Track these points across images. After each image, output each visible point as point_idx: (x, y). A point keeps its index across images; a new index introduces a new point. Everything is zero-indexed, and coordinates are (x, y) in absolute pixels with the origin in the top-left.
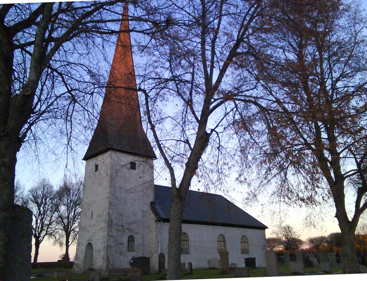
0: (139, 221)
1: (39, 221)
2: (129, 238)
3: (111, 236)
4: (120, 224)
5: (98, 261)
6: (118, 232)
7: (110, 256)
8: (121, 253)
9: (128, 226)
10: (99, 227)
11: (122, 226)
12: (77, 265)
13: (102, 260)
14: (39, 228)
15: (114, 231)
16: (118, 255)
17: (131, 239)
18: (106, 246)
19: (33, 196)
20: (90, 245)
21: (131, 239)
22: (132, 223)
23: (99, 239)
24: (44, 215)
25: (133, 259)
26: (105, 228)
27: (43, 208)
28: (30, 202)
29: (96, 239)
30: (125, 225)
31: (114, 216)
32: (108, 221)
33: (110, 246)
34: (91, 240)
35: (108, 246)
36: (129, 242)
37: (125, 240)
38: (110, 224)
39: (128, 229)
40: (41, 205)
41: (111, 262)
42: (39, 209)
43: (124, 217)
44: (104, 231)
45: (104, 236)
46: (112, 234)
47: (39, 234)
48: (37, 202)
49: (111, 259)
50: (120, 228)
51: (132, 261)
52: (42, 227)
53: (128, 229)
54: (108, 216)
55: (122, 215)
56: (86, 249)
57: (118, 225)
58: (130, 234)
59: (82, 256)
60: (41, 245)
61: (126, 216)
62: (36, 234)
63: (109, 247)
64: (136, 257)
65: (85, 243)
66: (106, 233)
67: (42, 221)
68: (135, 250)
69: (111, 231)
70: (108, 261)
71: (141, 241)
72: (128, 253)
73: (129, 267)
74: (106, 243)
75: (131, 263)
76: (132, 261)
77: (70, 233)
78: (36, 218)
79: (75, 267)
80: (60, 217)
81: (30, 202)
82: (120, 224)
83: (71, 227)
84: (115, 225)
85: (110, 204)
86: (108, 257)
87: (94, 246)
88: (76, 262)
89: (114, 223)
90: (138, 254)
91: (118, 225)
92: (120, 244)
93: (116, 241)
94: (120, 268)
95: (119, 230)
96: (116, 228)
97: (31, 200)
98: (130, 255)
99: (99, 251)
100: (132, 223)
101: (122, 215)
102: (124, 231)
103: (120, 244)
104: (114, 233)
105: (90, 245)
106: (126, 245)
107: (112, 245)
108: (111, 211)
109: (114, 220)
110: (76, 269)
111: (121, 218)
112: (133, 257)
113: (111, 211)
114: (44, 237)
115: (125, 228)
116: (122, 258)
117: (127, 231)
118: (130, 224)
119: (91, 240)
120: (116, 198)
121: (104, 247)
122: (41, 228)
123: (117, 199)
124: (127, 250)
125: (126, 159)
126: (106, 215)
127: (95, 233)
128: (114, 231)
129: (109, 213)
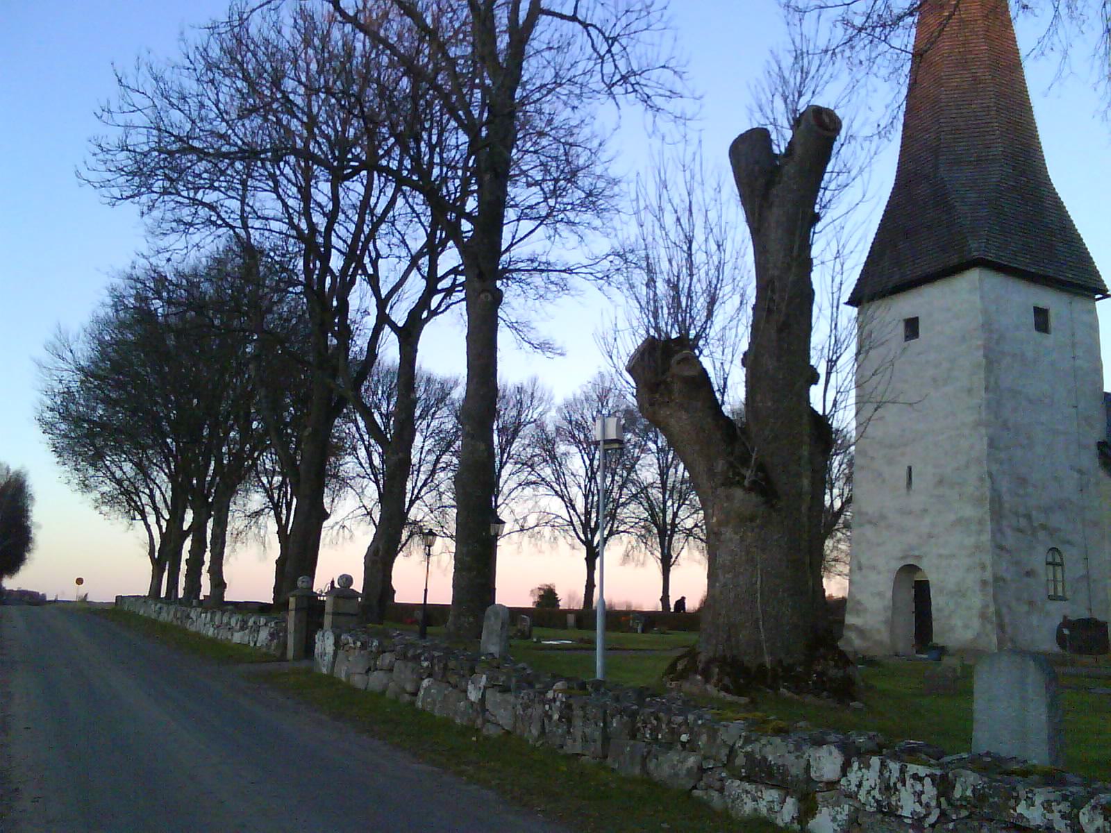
3: (1000, 548)
4: (1021, 510)
7: (1004, 610)
8: (1031, 603)
11: (1028, 517)
13: (976, 623)
15: (1008, 532)
16: (1026, 608)
18: (988, 575)
23: (953, 556)
25: (1066, 623)
26: (981, 522)
30: (1034, 513)
31: (1004, 485)
32: (992, 501)
33: (1004, 580)
35: (997, 579)
37: (1038, 560)
38: (997, 510)
39: (1043, 527)
41: (1009, 629)
43: (1030, 490)
44: (980, 532)
45: (978, 547)
46: (1004, 544)
49: (1007, 620)
50: (1023, 522)
53: (1043, 527)
54: (988, 483)
55: (1022, 481)
57: (1017, 514)
61: (1035, 486)
63: (1001, 584)
66: (986, 537)
68: (1068, 595)
69: (1000, 531)
70: (1001, 627)
72: (1053, 607)
73: (1056, 648)
74: (989, 569)
75: (1061, 639)
82: (1021, 510)
85: (992, 444)
86: (998, 614)
89: (1007, 506)
90: (1078, 611)
91: (1017, 514)
95: (1020, 530)
98: (1057, 612)
99: (960, 593)
104: (1010, 540)
107: (1008, 576)
108: (994, 468)
109: (1006, 498)
111: (1022, 492)
112: (1065, 617)
113: (994, 468)
116: (1035, 620)
117: (1042, 535)
118: (1047, 510)
120: (1005, 426)
121: (984, 583)
123: (1008, 429)
126: (982, 480)
127: (930, 536)
128: (1008, 532)
129: (990, 475)
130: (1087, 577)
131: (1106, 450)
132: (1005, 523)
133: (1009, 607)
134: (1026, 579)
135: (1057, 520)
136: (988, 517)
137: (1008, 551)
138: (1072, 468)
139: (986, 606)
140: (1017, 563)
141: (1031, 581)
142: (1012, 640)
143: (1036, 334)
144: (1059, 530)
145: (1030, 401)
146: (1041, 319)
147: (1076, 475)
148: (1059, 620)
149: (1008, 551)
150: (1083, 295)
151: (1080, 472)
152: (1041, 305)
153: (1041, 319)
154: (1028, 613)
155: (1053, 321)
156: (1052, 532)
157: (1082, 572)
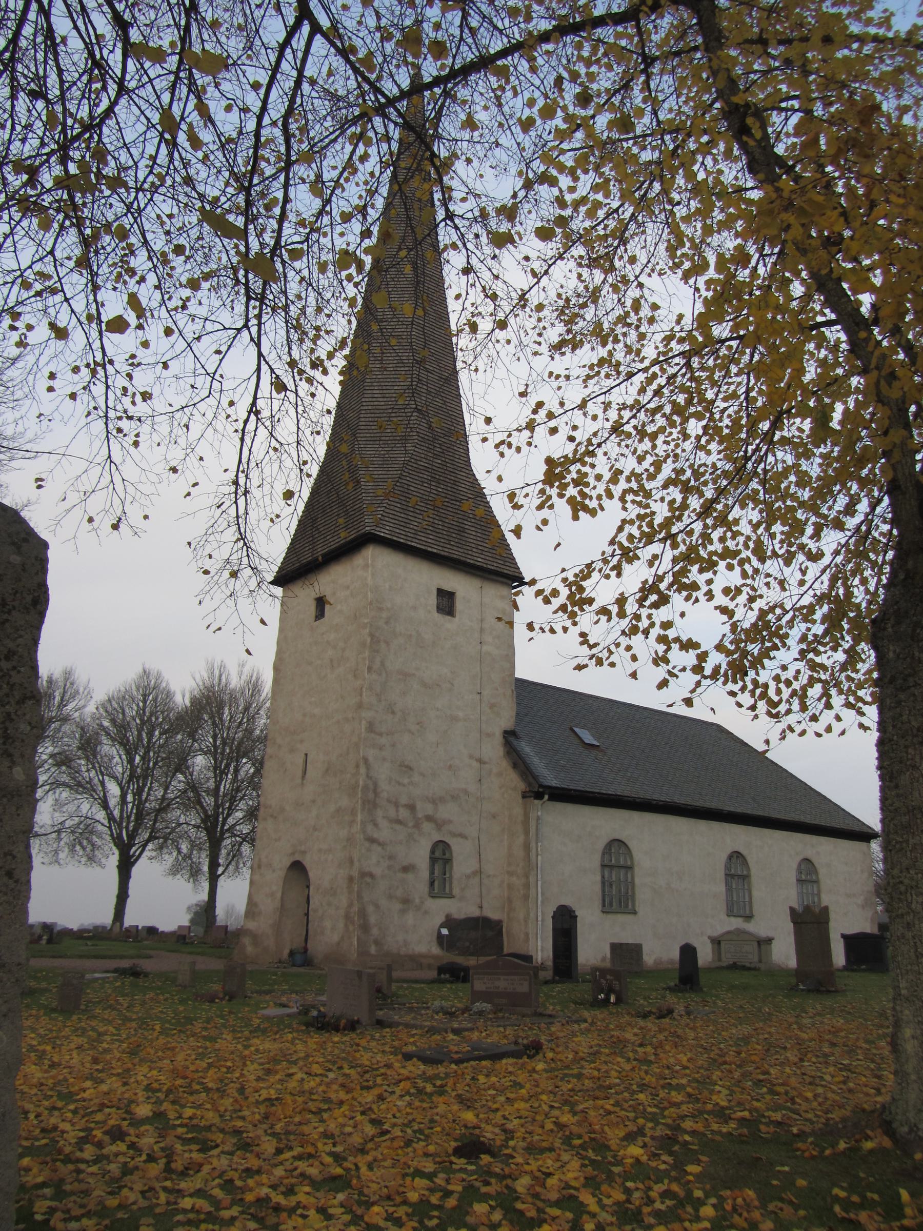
0: (466, 792)
1: (130, 798)
2: (433, 852)
3: (372, 840)
5: (328, 924)
6: (398, 827)
7: (370, 909)
8: (406, 901)
9: (429, 809)
10: (332, 808)
11: (412, 808)
12: (256, 938)
14: (129, 817)
15: (383, 824)
16: (397, 906)
17: (441, 855)
19: (113, 721)
20: (298, 868)
21: (441, 855)
22: (442, 800)
24: (145, 778)
25: (449, 922)
27: (143, 758)
28: (104, 740)
29: (320, 851)
30: (419, 806)
33: (371, 875)
34: (304, 853)
36: (433, 860)
37: (420, 855)
39: (429, 818)
40: (136, 749)
41: (375, 931)
42: (131, 761)
47: (132, 836)
48: (123, 743)
49: (373, 919)
50: (404, 813)
51: (445, 931)
52: (140, 816)
53: (429, 818)
55: (407, 768)
56: (286, 880)
57: (397, 805)
58: (437, 837)
59: (268, 906)
60: (136, 870)
62: (120, 835)
63: (368, 879)
64: (456, 916)
65: (282, 862)
67: (140, 795)
68: (456, 891)
69: (376, 825)
71: (473, 865)
72: (431, 904)
73: (436, 950)
75: (440, 936)
76: (445, 931)
77: (222, 839)
78: (122, 789)
79: (246, 941)
80: (193, 786)
81: (104, 740)
82: (404, 800)
83: (225, 820)
84: (389, 801)
87: (311, 874)
88: (251, 925)
90: (463, 907)
92: (406, 869)
93: (391, 857)
94: (403, 951)
95: (399, 822)
96: (392, 812)
97: (108, 734)
98: (439, 910)
100: (442, 800)
101: (411, 769)
102: (417, 826)
103: (406, 869)
104: (385, 832)
105: (298, 868)
106: (425, 874)
107: (377, 871)
109: (384, 786)
110: (250, 949)
111: (406, 781)
114: (144, 847)
115: (420, 815)
116: (410, 919)
117: (427, 826)
118: (435, 801)
119: (304, 853)
121: (351, 879)
122: (136, 820)
124: (427, 889)
125: (425, 579)
128: (383, 824)
130: (479, 872)
131: (512, 739)
132: (379, 813)
133: (377, 906)
134: (400, 875)
135: (444, 812)
136: (359, 807)
137: (381, 844)
138: (471, 757)
139: (351, 905)
140: (391, 857)
141: (410, 876)
142: (377, 942)
143: (437, 616)
144: (450, 822)
145: (424, 685)
146: (446, 602)
147: (475, 764)
148: (441, 919)
149: (381, 844)
150: (502, 583)
151: (480, 761)
152: (447, 587)
153: (446, 602)
154: (403, 912)
155: (459, 605)
156: (439, 825)
157: (476, 867)
